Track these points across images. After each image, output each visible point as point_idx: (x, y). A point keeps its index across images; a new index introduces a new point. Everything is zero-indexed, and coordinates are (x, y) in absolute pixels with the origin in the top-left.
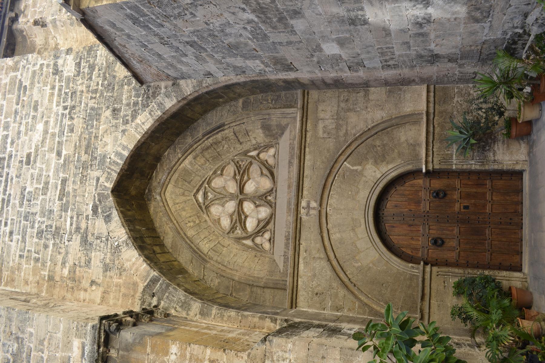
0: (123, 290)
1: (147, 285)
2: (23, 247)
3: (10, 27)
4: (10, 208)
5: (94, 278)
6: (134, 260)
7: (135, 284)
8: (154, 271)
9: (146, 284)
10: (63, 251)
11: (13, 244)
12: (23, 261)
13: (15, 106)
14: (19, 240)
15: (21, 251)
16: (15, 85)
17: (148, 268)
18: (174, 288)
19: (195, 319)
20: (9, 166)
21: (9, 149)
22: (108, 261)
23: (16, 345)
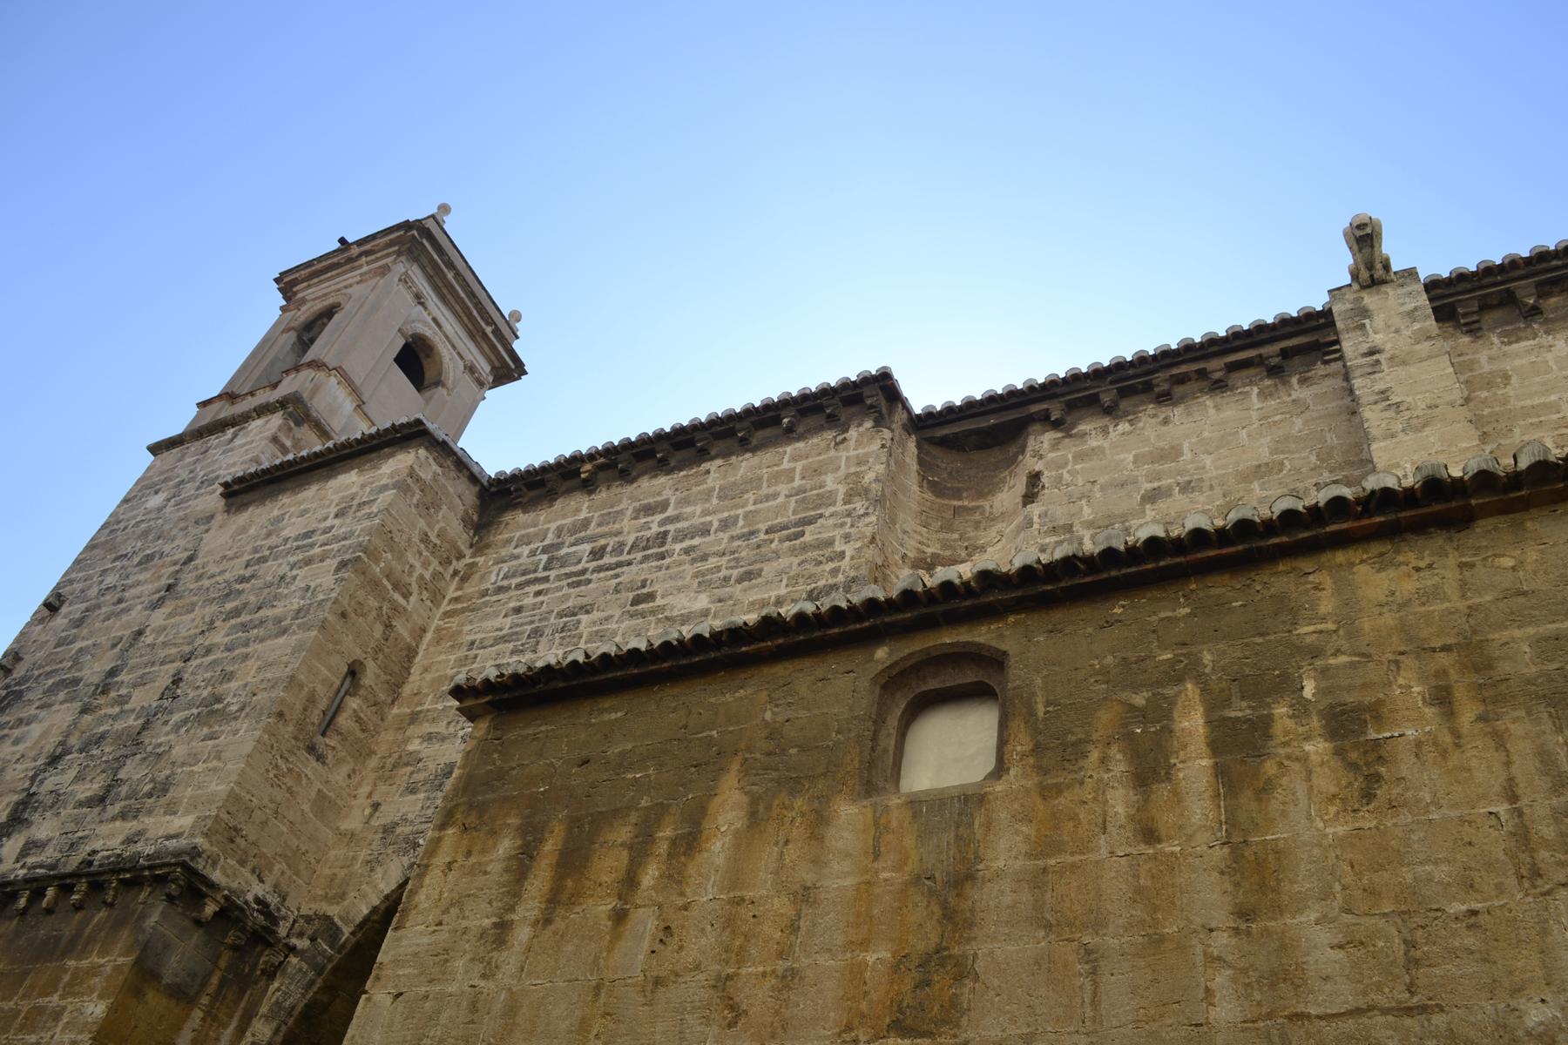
0: (342, 873)
1: (333, 923)
2: (486, 643)
3: (1031, 419)
4: (566, 590)
5: (382, 808)
6: (382, 886)
7: (342, 896)
8: (353, 933)
9: (336, 920)
10: (451, 730)
11: (497, 622)
12: (461, 653)
13: (763, 527)
14: (500, 629)
15: (482, 640)
16: (809, 509)
17: (359, 920)
18: (312, 982)
19: (248, 1034)
20: (646, 559)
21: (678, 547)
22: (399, 830)
23: (234, 708)
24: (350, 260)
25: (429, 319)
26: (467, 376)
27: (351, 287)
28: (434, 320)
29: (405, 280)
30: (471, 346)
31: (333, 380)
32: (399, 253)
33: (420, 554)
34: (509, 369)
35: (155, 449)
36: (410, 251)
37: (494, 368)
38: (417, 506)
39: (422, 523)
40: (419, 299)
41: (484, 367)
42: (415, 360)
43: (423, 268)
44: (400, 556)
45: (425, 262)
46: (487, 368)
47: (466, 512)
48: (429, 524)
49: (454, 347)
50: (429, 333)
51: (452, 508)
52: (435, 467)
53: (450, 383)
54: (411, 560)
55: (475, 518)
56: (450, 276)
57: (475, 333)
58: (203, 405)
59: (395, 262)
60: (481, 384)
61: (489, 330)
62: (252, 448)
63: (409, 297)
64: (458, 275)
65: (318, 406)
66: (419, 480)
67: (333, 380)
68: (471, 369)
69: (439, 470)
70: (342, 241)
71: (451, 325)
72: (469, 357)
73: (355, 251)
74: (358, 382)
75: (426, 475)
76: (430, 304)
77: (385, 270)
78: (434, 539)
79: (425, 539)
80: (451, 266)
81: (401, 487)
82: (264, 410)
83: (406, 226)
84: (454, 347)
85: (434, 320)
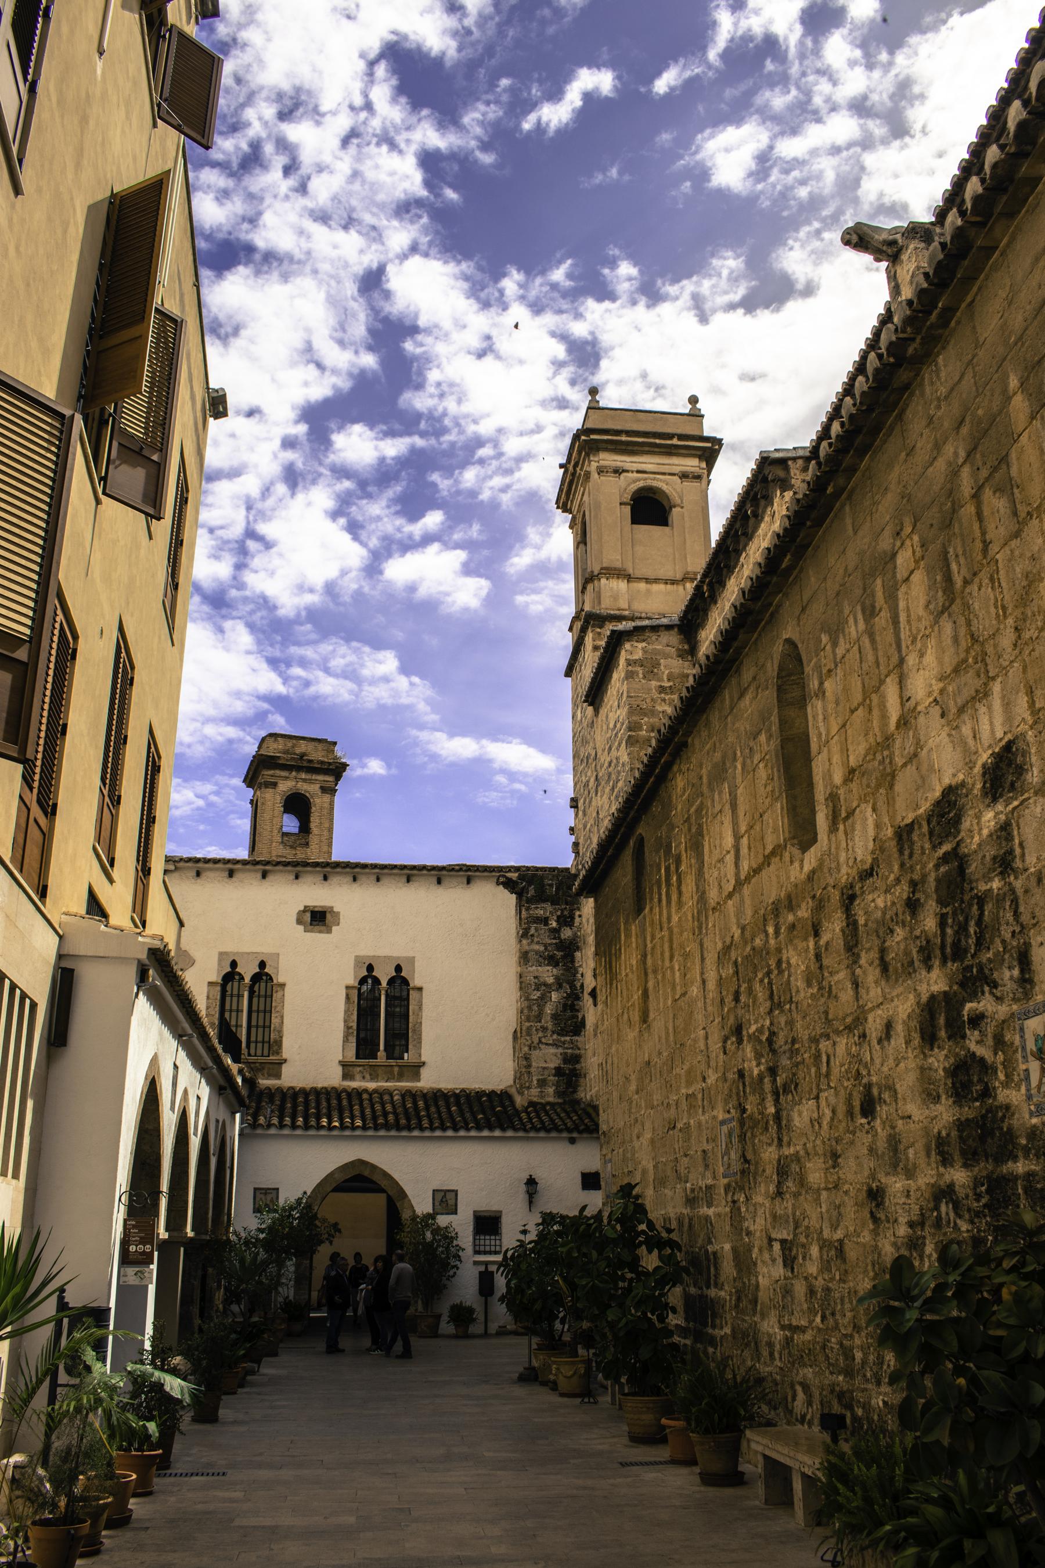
24: (573, 474)
25: (635, 475)
26: (687, 484)
27: (584, 496)
28: (638, 472)
29: (601, 471)
30: (675, 460)
31: (603, 581)
32: (588, 455)
33: (664, 700)
34: (709, 451)
35: (569, 672)
36: (591, 449)
37: (700, 458)
38: (644, 677)
39: (654, 683)
40: (618, 471)
41: (692, 464)
42: (649, 508)
43: (606, 450)
44: (652, 712)
45: (604, 445)
46: (695, 462)
47: (678, 650)
48: (659, 680)
49: (664, 474)
50: (641, 484)
51: (667, 656)
52: (640, 645)
53: (678, 501)
54: (659, 708)
55: (686, 647)
56: (624, 438)
57: (670, 451)
58: (571, 629)
59: (590, 462)
60: (698, 477)
61: (675, 441)
62: (590, 660)
63: (611, 479)
64: (628, 433)
65: (607, 606)
66: (635, 662)
67: (603, 581)
68: (684, 476)
69: (644, 644)
70: (561, 466)
71: (649, 462)
72: (677, 470)
73: (571, 468)
74: (618, 565)
75: (638, 655)
76: (627, 466)
77: (588, 475)
78: (667, 684)
79: (662, 689)
80: (618, 432)
81: (630, 676)
82: (584, 630)
83: (576, 437)
84: (664, 474)
85: (638, 472)
